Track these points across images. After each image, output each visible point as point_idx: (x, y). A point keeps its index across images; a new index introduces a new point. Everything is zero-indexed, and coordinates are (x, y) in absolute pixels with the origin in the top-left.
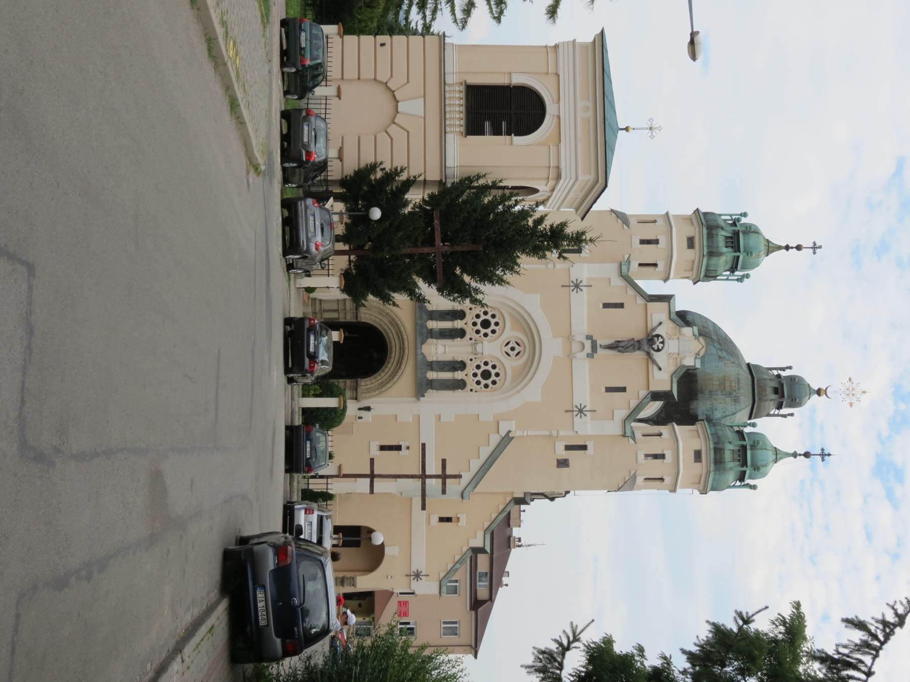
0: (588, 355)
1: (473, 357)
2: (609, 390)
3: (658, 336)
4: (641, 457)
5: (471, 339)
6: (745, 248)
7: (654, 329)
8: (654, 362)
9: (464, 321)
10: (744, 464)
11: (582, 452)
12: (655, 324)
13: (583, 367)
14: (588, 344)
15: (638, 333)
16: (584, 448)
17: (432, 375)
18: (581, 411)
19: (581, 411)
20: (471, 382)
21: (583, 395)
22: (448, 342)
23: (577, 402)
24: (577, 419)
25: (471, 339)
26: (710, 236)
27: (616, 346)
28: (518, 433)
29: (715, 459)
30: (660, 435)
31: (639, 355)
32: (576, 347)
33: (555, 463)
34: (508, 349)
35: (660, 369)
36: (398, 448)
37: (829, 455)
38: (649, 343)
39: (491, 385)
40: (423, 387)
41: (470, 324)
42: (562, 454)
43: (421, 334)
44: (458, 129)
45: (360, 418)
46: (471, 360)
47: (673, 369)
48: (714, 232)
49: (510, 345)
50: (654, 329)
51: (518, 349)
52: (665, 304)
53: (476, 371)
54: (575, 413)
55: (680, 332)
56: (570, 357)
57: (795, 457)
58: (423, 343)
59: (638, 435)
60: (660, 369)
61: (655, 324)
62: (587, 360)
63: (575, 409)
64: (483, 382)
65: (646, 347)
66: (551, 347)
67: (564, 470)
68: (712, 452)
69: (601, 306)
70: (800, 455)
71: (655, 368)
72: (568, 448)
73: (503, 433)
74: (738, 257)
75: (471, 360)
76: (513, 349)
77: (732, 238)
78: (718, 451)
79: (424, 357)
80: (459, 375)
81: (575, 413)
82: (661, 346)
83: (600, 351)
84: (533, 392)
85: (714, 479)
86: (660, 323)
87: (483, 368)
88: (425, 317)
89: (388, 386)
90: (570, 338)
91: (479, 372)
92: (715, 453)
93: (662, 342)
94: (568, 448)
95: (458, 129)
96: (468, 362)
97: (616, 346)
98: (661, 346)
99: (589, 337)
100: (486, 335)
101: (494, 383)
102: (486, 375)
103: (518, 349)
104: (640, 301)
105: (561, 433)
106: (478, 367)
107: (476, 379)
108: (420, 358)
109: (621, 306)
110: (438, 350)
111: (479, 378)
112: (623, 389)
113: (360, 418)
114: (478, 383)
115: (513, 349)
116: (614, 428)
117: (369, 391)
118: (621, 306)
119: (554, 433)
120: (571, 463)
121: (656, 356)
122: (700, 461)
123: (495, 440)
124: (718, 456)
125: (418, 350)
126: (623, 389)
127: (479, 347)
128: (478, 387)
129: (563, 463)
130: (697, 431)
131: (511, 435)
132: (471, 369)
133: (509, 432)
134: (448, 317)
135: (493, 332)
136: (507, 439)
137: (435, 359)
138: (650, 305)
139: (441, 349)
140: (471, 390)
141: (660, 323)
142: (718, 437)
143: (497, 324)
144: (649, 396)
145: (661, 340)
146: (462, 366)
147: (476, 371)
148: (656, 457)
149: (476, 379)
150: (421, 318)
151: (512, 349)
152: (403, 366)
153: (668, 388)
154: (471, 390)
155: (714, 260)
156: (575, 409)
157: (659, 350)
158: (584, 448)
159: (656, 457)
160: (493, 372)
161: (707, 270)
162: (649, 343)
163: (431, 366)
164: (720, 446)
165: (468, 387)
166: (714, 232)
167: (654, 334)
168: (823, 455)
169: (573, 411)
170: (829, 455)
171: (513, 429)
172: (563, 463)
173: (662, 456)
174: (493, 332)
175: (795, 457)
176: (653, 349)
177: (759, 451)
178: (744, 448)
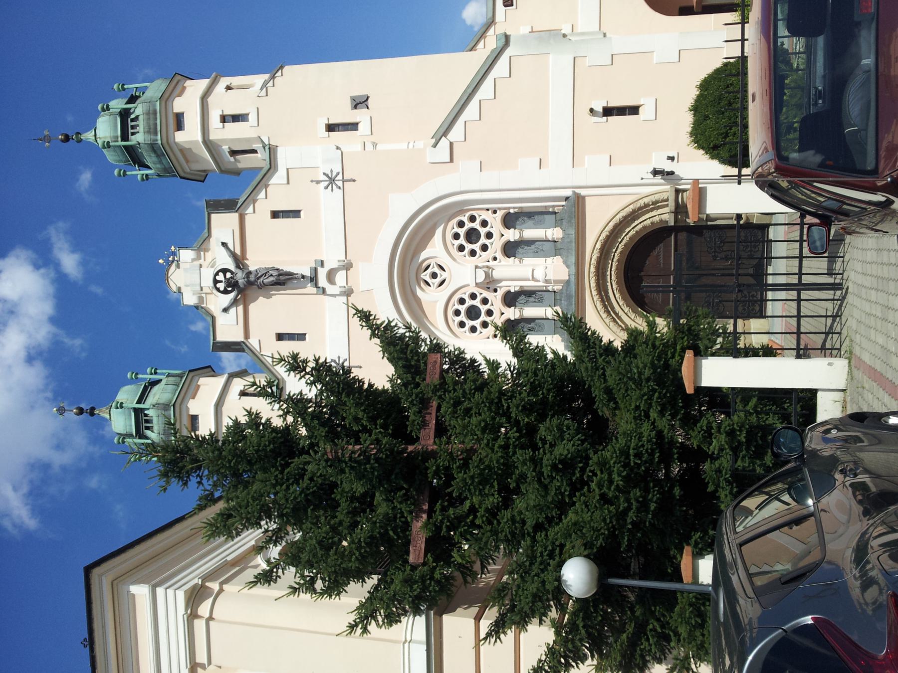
1: (492, 263)
2: (296, 214)
3: (225, 292)
4: (252, 118)
6: (130, 415)
8: (233, 255)
14: (322, 281)
16: (331, 128)
18: (332, 180)
20: (496, 224)
29: (156, 119)
31: (254, 263)
34: (442, 275)
35: (224, 244)
36: (608, 112)
41: (496, 314)
45: (672, 158)
46: (495, 259)
50: (235, 303)
52: (220, 338)
53: (488, 242)
55: (201, 299)
58: (568, 282)
60: (224, 244)
61: (233, 310)
67: (359, 92)
71: (231, 246)
72: (353, 126)
73: (444, 143)
74: (139, 402)
75: (495, 259)
77: (147, 428)
79: (565, 262)
80: (512, 235)
81: (340, 177)
82: (221, 277)
84: (401, 208)
87: (477, 247)
89: (623, 214)
91: (483, 240)
93: (216, 282)
94: (353, 126)
96: (499, 255)
98: (221, 277)
102: (472, 236)
104: (253, 342)
105: (360, 147)
106: (485, 248)
108: (573, 259)
111: (483, 231)
112: (275, 215)
113: (672, 158)
114: (484, 223)
115: (434, 276)
116: (284, 159)
117: (656, 205)
119: (369, 147)
120: (348, 104)
121: (230, 265)
123: (456, 133)
124: (152, 122)
125: (573, 269)
126: (275, 215)
127: (481, 277)
129: (360, 103)
130: (187, 161)
131: (434, 140)
132: (496, 245)
133: (435, 146)
135: (462, 301)
137: (549, 260)
138: (238, 337)
139: (539, 275)
140: (495, 212)
141: (225, 310)
145: (221, 286)
146: (510, 249)
148: (236, 118)
152: (598, 246)
153: (214, 217)
157: (224, 271)
158: (331, 128)
159: (236, 118)
160: (462, 241)
163: (555, 248)
165: (500, 214)
171: (430, 149)
172: (360, 103)
173: (224, 119)
174: (462, 301)
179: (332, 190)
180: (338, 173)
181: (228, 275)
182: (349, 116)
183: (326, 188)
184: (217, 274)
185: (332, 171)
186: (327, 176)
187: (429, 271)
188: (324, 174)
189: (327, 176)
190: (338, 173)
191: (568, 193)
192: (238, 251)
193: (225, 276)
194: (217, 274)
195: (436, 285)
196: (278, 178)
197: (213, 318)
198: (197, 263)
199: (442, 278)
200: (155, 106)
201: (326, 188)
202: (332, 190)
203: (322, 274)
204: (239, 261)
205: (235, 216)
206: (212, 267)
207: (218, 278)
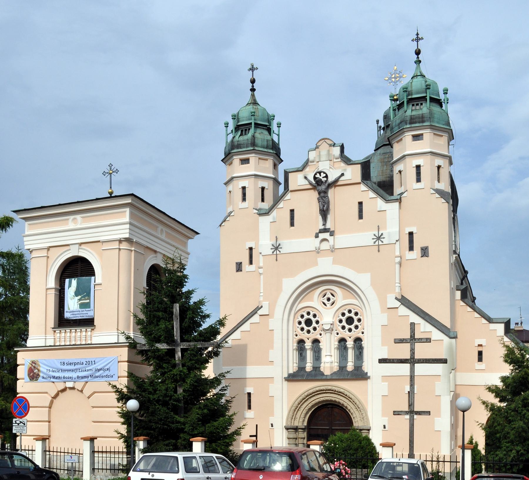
0: (332, 234)
3: (315, 178)
5: (321, 335)
7: (311, 184)
8: (337, 180)
9: (306, 340)
10: (424, 98)
11: (415, 236)
12: (307, 183)
13: (341, 240)
14: (322, 236)
15: (314, 195)
17: (350, 366)
18: (379, 238)
19: (379, 238)
20: (356, 333)
21: (366, 238)
22: (323, 353)
23: (371, 242)
24: (385, 241)
25: (321, 335)
26: (239, 146)
27: (324, 213)
28: (397, 290)
30: (400, 172)
32: (325, 246)
33: (425, 258)
35: (343, 175)
37: (417, 34)
38: (322, 186)
39: (358, 317)
40: (359, 375)
42: (416, 253)
43: (316, 375)
44: (89, 333)
46: (338, 334)
47: (343, 164)
48: (236, 143)
49: (326, 302)
51: (329, 295)
52: (291, 175)
54: (380, 243)
56: (333, 250)
57: (420, 62)
59: (402, 190)
60: (343, 175)
62: (336, 236)
63: (377, 243)
64: (356, 323)
65: (323, 187)
66: (326, 266)
68: (413, 125)
69: (293, 228)
70: (418, 58)
72: (411, 248)
73: (398, 304)
76: (329, 299)
78: (413, 120)
80: (350, 343)
81: (380, 243)
82: (323, 175)
83: (328, 226)
84: (362, 280)
85: (438, 123)
86: (306, 178)
87: (344, 323)
88: (302, 373)
90: (318, 251)
91: (347, 327)
94: (411, 248)
95: (89, 333)
96: (340, 336)
97: (324, 213)
98: (323, 175)
99: (317, 236)
100: (317, 322)
101: (356, 314)
102: (350, 321)
103: (329, 295)
104: (289, 196)
105: (398, 253)
106: (343, 328)
107: (353, 329)
109: (292, 211)
110: (329, 362)
112: (360, 203)
115: (329, 299)
118: (292, 211)
119: (398, 260)
120: (424, 245)
121: (331, 179)
122: (422, 135)
123: (403, 311)
126: (360, 203)
128: (360, 327)
129: (425, 252)
132: (345, 334)
133: (396, 298)
134: (303, 354)
136: (404, 301)
138: (291, 188)
140: (363, 333)
142: (401, 122)
143: (308, 313)
144: (365, 182)
145: (318, 176)
147: (346, 329)
148: (418, 174)
149: (353, 329)
150: (303, 376)
151: (329, 300)
154: (363, 333)
155: (259, 142)
156: (377, 243)
157: (326, 177)
159: (418, 174)
161: (267, 147)
162: (322, 186)
165: (360, 335)
166: (236, 143)
167: (314, 182)
168: (418, 39)
169: (379, 245)
170: (417, 34)
172: (425, 252)
173: (418, 167)
174: (315, 316)
175: (420, 62)
176: (326, 181)
177: (413, 88)
178: (410, 101)
179: (373, 239)
180: (382, 242)
181: (325, 179)
182: (417, 245)
183: (375, 235)
184: (324, 173)
185: (384, 238)
186: (381, 236)
187: (331, 297)
188: (382, 234)
189: (381, 236)
190: (382, 242)
191: (369, 375)
192: (339, 183)
193: (323, 177)
194: (324, 173)
195: (324, 301)
196: (380, 203)
197: (302, 171)
199: (327, 304)
200: (428, 121)
201: (375, 235)
202: (373, 239)
203: (326, 235)
204: (334, 184)
205: (359, 180)
206: (330, 167)
207: (322, 174)
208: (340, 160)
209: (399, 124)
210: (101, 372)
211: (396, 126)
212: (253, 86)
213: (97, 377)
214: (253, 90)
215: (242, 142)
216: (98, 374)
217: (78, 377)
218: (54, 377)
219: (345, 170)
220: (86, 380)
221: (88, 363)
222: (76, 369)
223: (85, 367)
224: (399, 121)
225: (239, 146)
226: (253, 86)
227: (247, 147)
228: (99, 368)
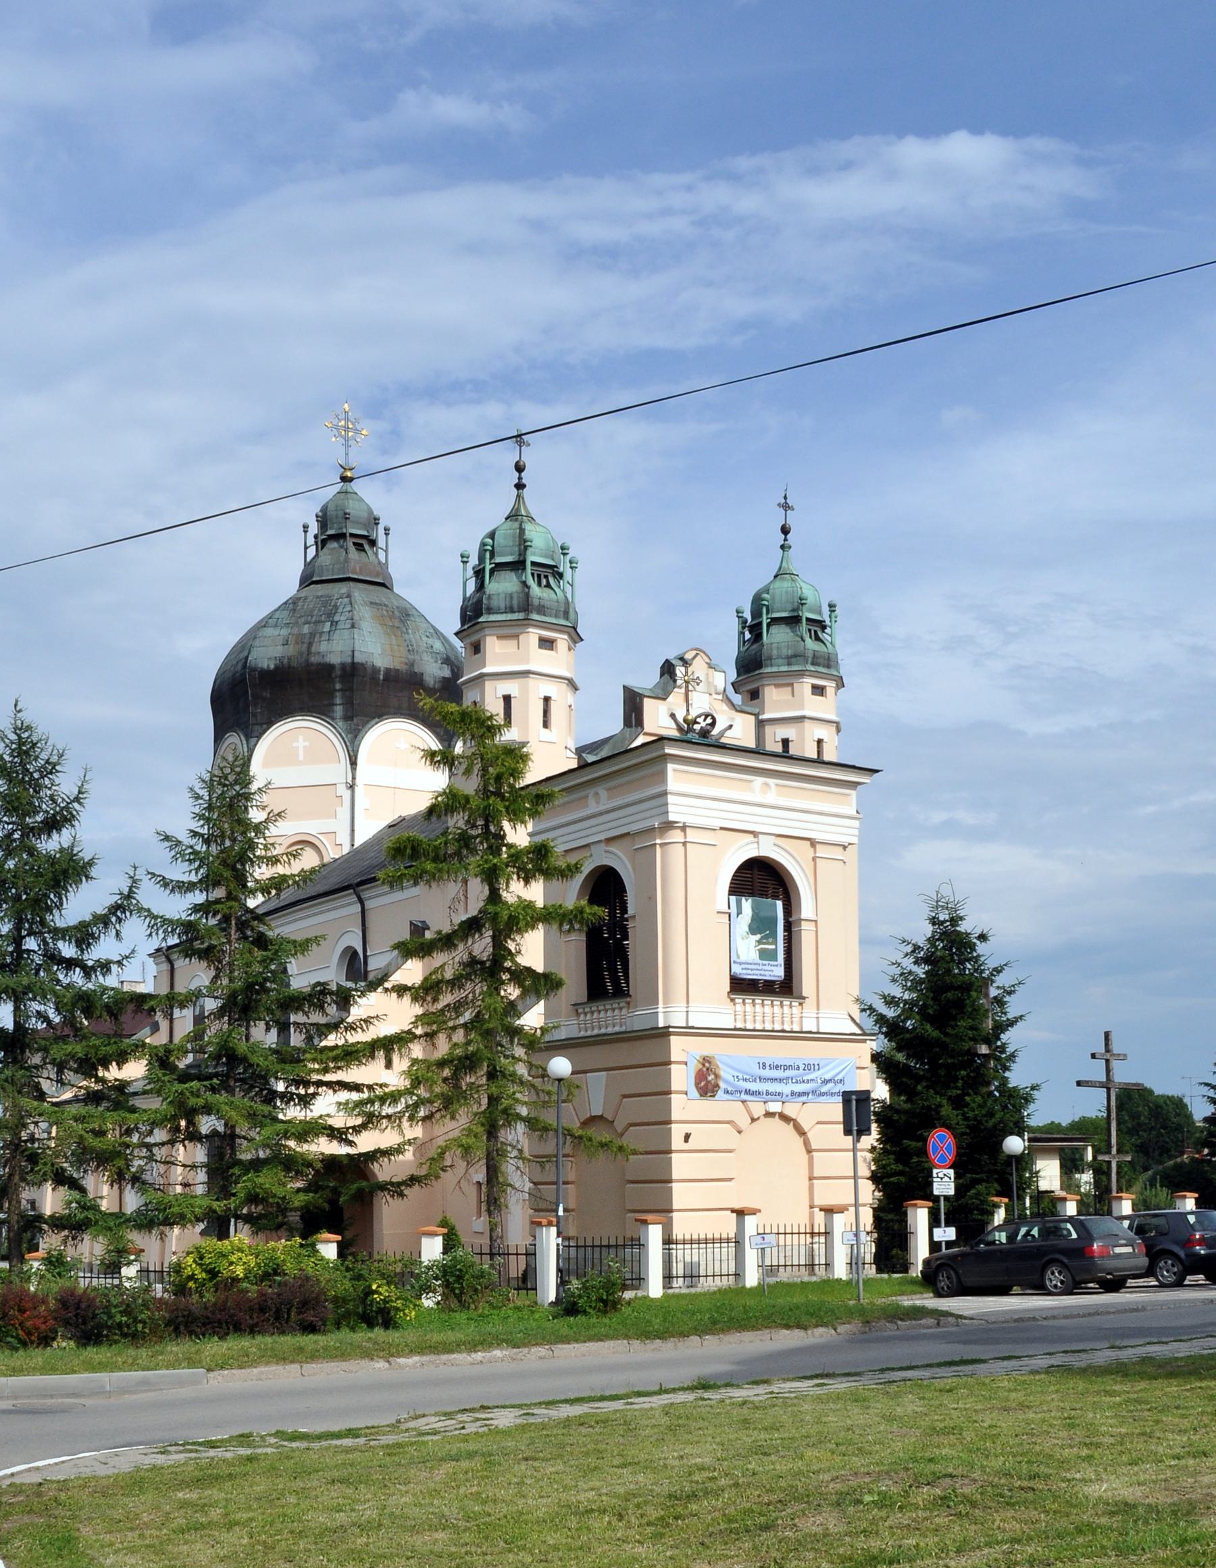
12: (674, 726)
26: (541, 610)
92: (818, 665)
98: (709, 720)
124: (821, 661)
142: (795, 656)
164: (810, 655)
175: (782, 547)
198: (713, 692)
208: (720, 697)
209: (788, 658)
210: (830, 1085)
211: (779, 657)
212: (520, 478)
213: (823, 1094)
214: (520, 486)
215: (547, 604)
216: (824, 1089)
217: (793, 1093)
218: (747, 1092)
219: (733, 719)
220: (804, 1098)
221: (809, 1067)
222: (787, 1078)
223: (802, 1075)
224: (790, 653)
225: (541, 610)
226: (520, 478)
227: (556, 616)
228: (828, 1077)
